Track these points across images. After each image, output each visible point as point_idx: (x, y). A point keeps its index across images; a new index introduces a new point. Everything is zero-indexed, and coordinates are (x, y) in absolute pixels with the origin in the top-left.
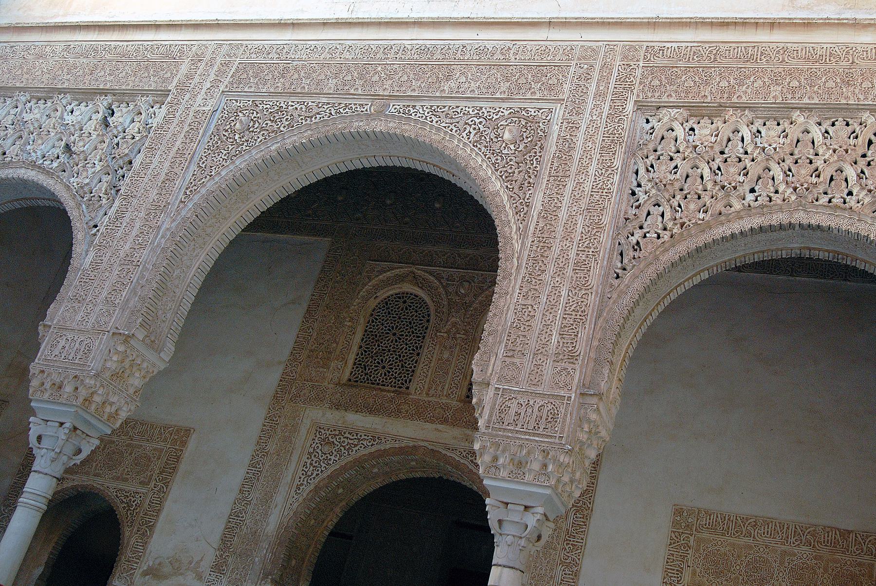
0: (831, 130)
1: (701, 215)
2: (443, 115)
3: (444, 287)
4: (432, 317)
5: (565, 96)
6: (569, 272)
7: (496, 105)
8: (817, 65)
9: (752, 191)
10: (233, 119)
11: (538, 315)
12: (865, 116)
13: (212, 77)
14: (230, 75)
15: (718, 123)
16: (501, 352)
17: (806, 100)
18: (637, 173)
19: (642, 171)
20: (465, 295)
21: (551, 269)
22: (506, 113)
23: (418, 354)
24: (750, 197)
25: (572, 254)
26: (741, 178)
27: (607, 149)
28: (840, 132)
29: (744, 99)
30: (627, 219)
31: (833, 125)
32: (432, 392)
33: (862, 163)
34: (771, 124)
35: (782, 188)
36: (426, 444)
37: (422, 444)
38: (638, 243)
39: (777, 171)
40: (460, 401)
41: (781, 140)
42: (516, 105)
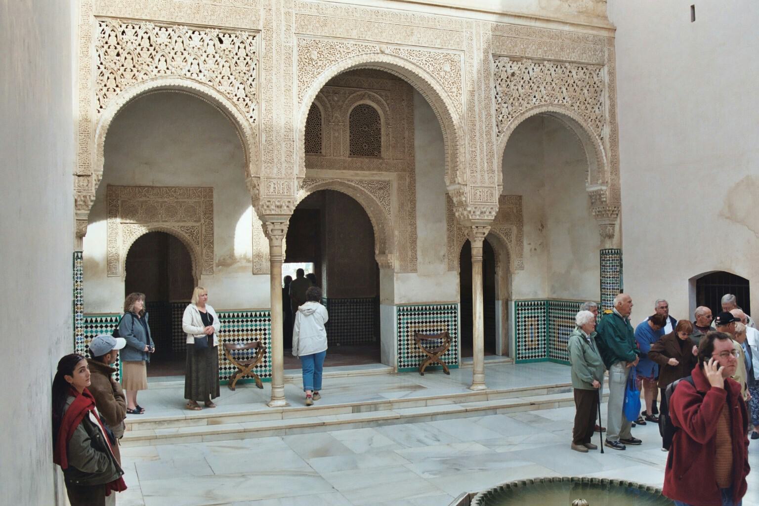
0: (557, 70)
1: (521, 108)
2: (414, 55)
3: (326, 97)
4: (322, 113)
5: (465, 49)
6: (485, 137)
7: (437, 51)
8: (552, 40)
9: (535, 97)
10: (307, 51)
11: (478, 155)
12: (567, 64)
13: (283, 23)
14: (294, 22)
15: (520, 63)
16: (468, 171)
17: (550, 57)
18: (495, 87)
19: (498, 87)
20: (338, 101)
21: (478, 134)
22: (442, 56)
23: (320, 134)
24: (534, 100)
25: (484, 127)
26: (531, 91)
27: (487, 77)
28: (559, 70)
29: (530, 55)
30: (497, 110)
31: (557, 68)
32: (335, 154)
33: (567, 85)
34: (537, 65)
35: (545, 96)
36: (338, 180)
37: (336, 180)
38: (501, 121)
39: (542, 88)
40: (349, 157)
41: (542, 74)
42: (445, 52)
